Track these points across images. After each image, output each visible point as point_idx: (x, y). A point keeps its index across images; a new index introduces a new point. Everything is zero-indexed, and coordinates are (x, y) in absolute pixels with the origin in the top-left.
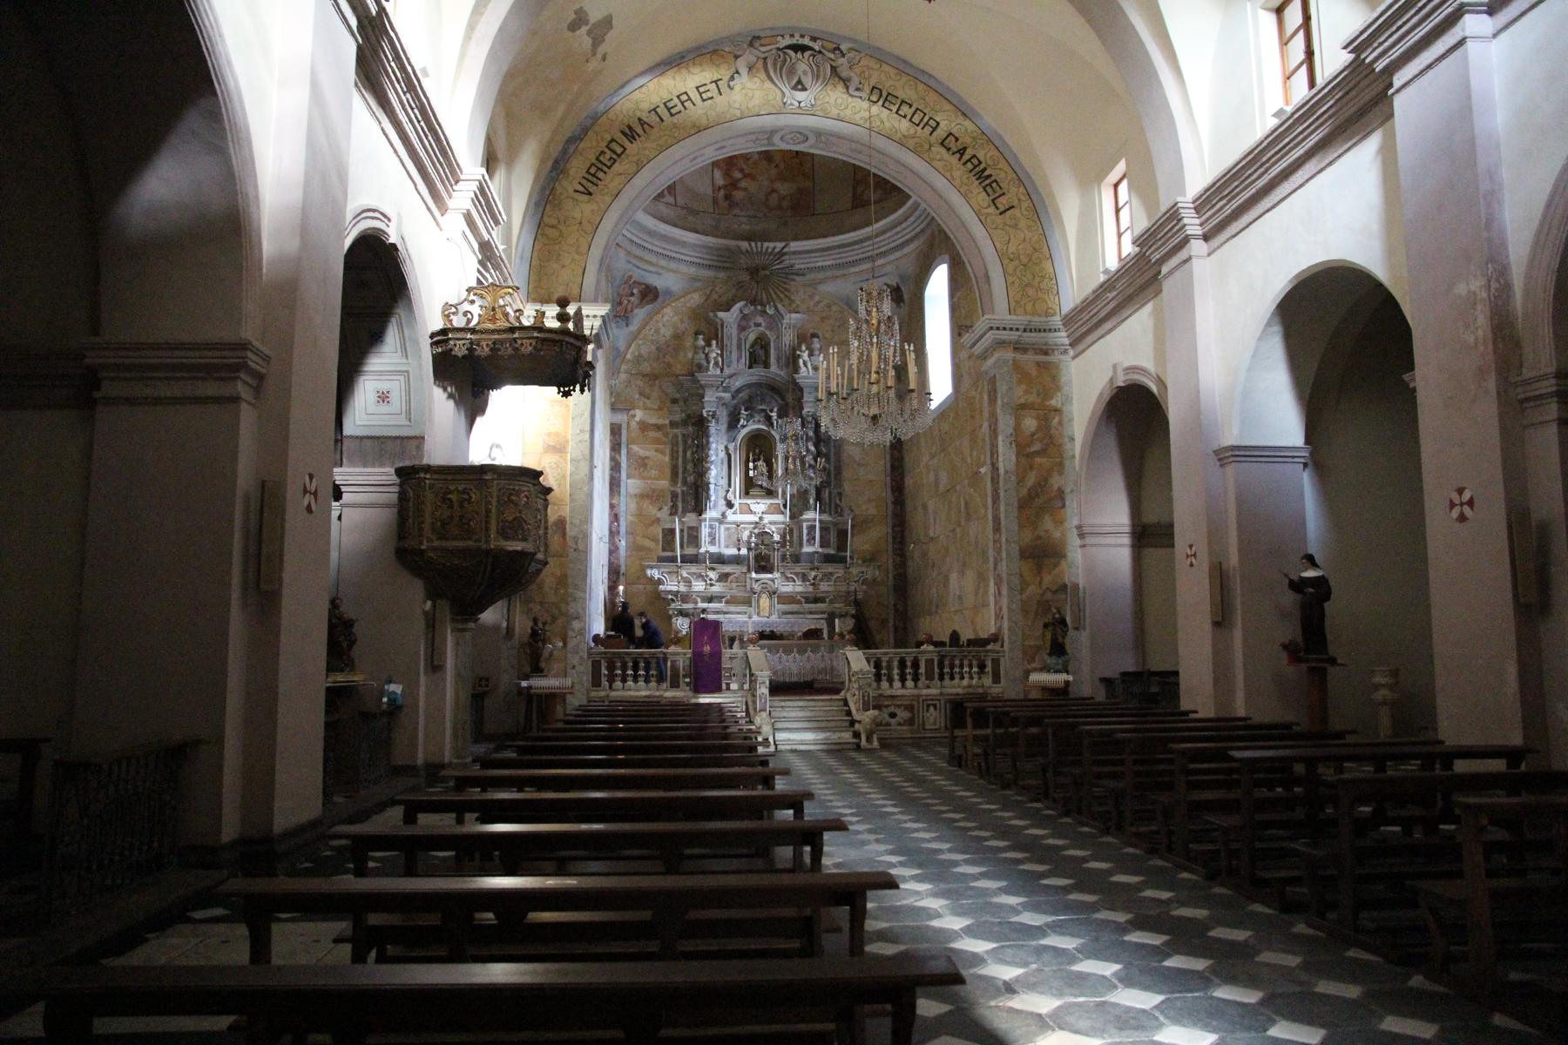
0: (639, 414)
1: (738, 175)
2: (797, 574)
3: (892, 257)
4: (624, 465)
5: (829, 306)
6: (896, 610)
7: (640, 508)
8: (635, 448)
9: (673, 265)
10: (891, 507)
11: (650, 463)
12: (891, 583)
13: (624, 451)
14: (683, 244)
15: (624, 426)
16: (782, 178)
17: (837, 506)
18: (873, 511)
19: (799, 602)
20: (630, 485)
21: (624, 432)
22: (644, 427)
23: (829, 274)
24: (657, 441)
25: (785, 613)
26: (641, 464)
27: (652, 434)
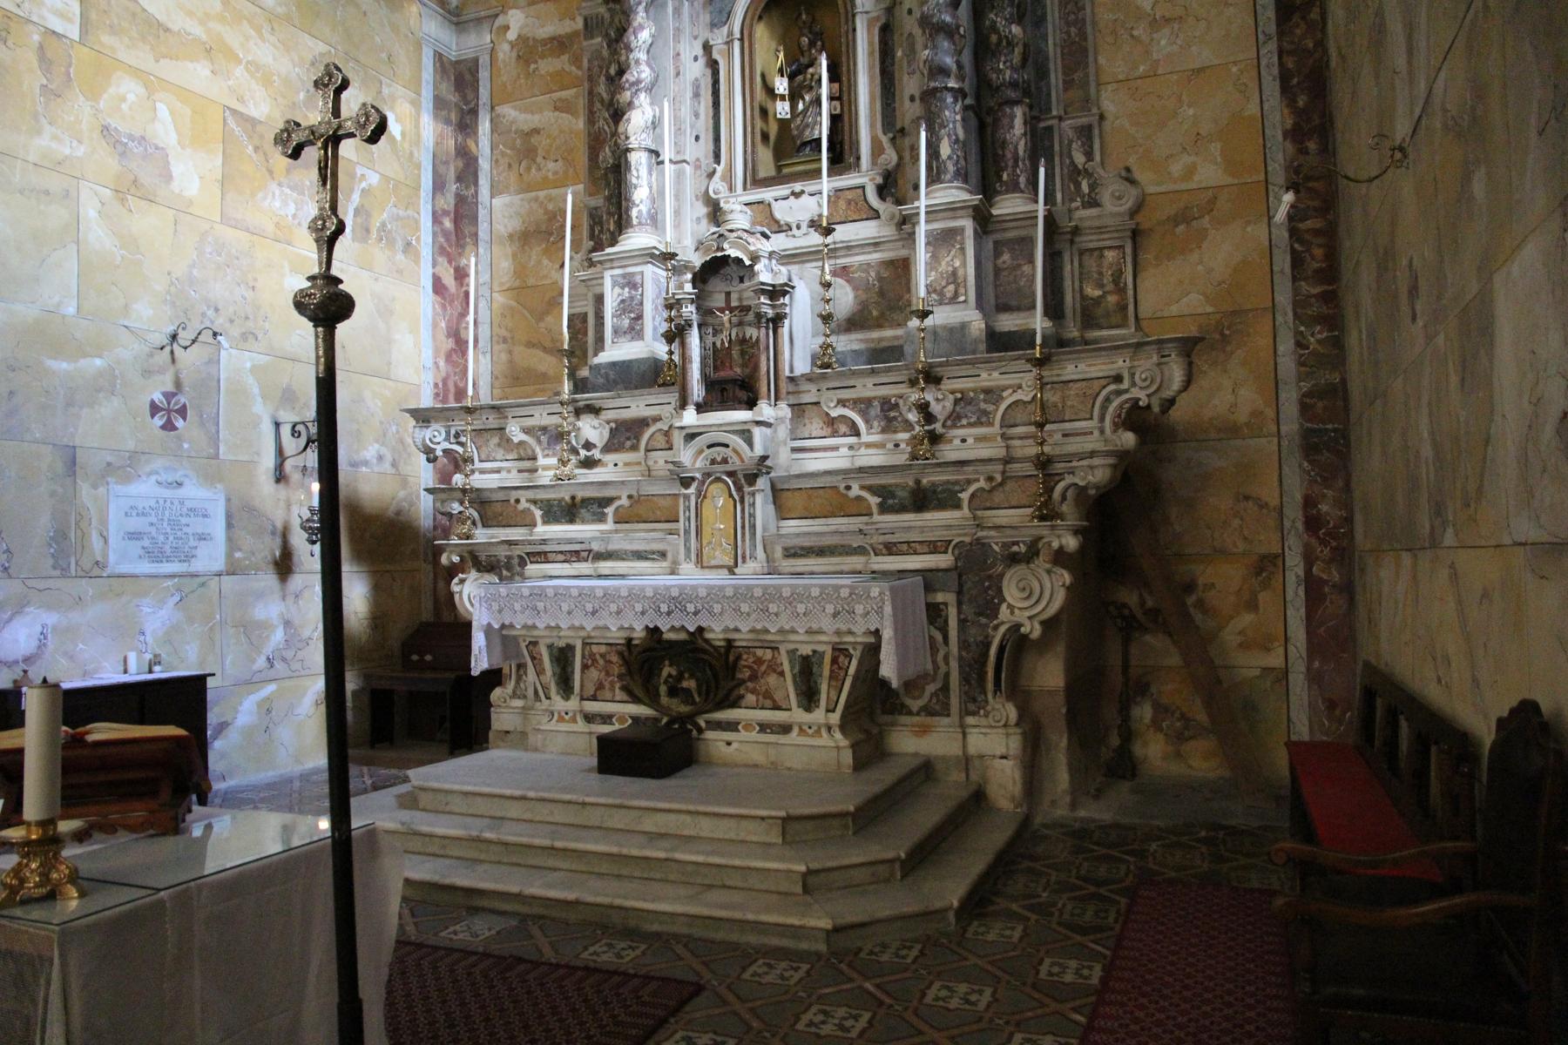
0: (516, 21)
2: (862, 405)
4: (484, 164)
6: (1313, 523)
7: (520, 271)
8: (508, 111)
10: (1280, 154)
11: (541, 142)
12: (1291, 424)
13: (484, 126)
15: (484, 60)
17: (1075, 173)
18: (1210, 174)
19: (856, 508)
20: (499, 210)
21: (484, 75)
22: (528, 50)
24: (560, 80)
25: (791, 553)
26: (524, 149)
27: (547, 66)
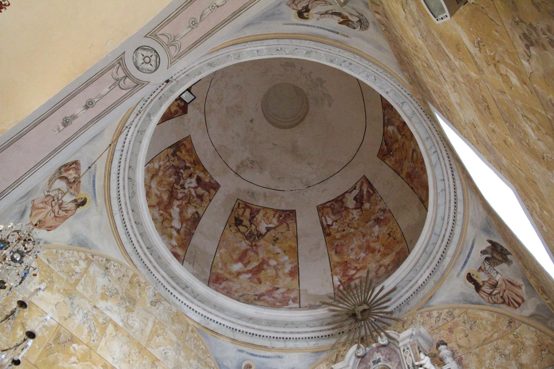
1: (353, 272)
3: (459, 217)
5: (451, 314)
9: (290, 344)
14: (293, 324)
16: (385, 255)
23: (431, 283)
